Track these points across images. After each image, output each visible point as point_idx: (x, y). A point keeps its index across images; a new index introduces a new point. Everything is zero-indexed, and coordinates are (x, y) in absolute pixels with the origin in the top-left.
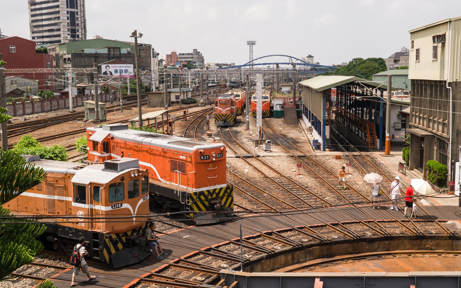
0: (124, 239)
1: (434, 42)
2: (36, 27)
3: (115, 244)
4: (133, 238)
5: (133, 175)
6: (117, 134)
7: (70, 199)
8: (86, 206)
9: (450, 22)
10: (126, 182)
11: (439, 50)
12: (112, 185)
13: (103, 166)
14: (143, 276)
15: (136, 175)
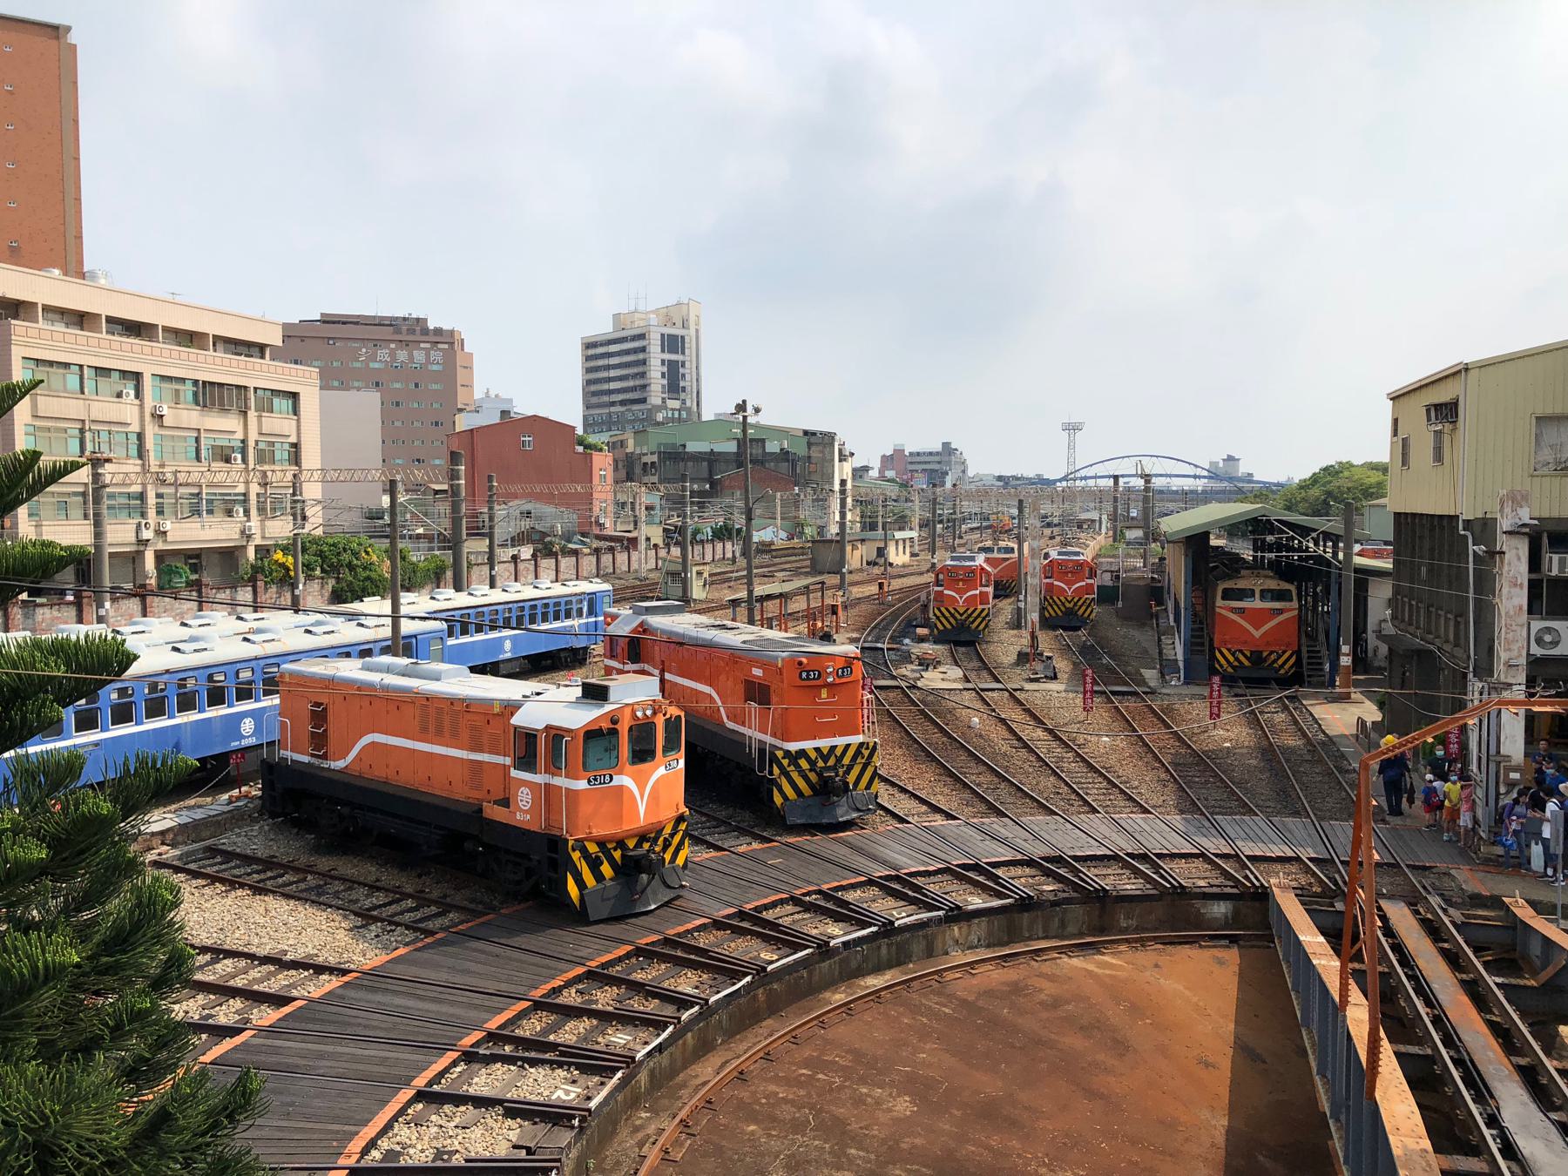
0: (617, 855)
1: (1429, 419)
2: (594, 394)
3: (594, 865)
4: (639, 852)
5: (639, 714)
6: (656, 621)
7: (508, 761)
8: (539, 778)
9: (1467, 370)
10: (623, 729)
11: (1446, 438)
12: (592, 734)
13: (578, 692)
14: (644, 941)
15: (649, 713)
